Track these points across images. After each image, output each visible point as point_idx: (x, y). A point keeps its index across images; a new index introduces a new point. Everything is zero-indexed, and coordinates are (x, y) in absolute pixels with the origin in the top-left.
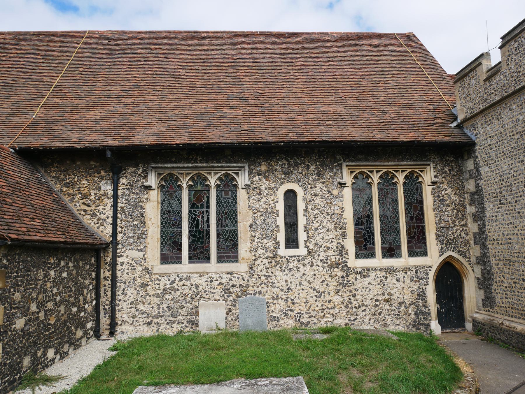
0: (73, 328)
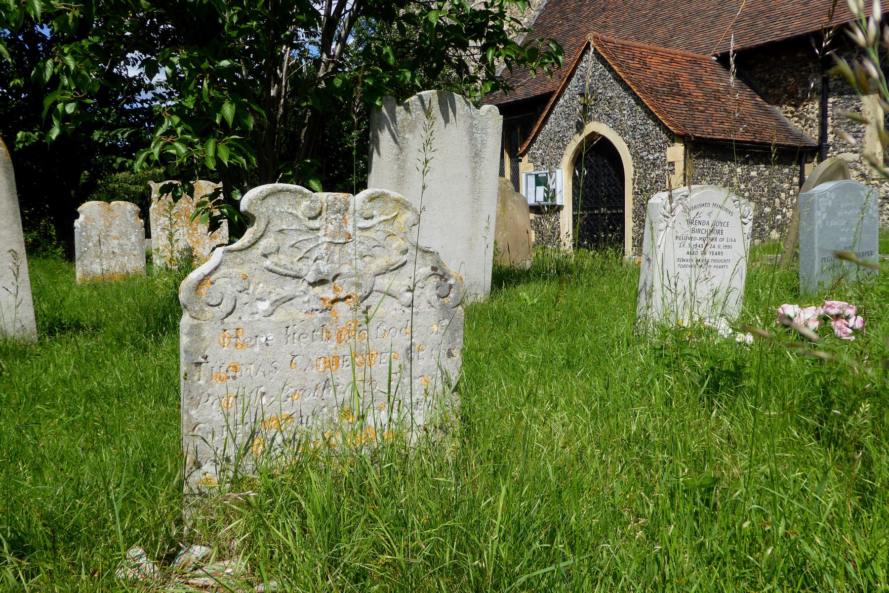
0: (767, 228)
